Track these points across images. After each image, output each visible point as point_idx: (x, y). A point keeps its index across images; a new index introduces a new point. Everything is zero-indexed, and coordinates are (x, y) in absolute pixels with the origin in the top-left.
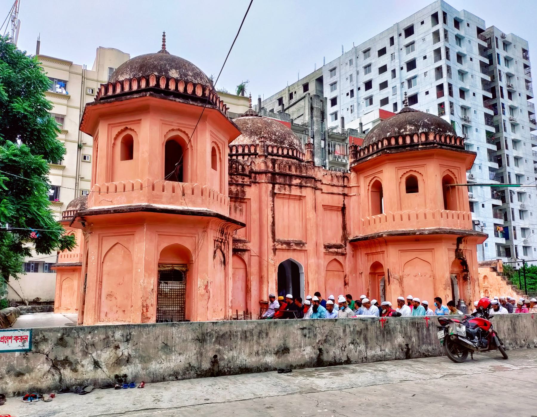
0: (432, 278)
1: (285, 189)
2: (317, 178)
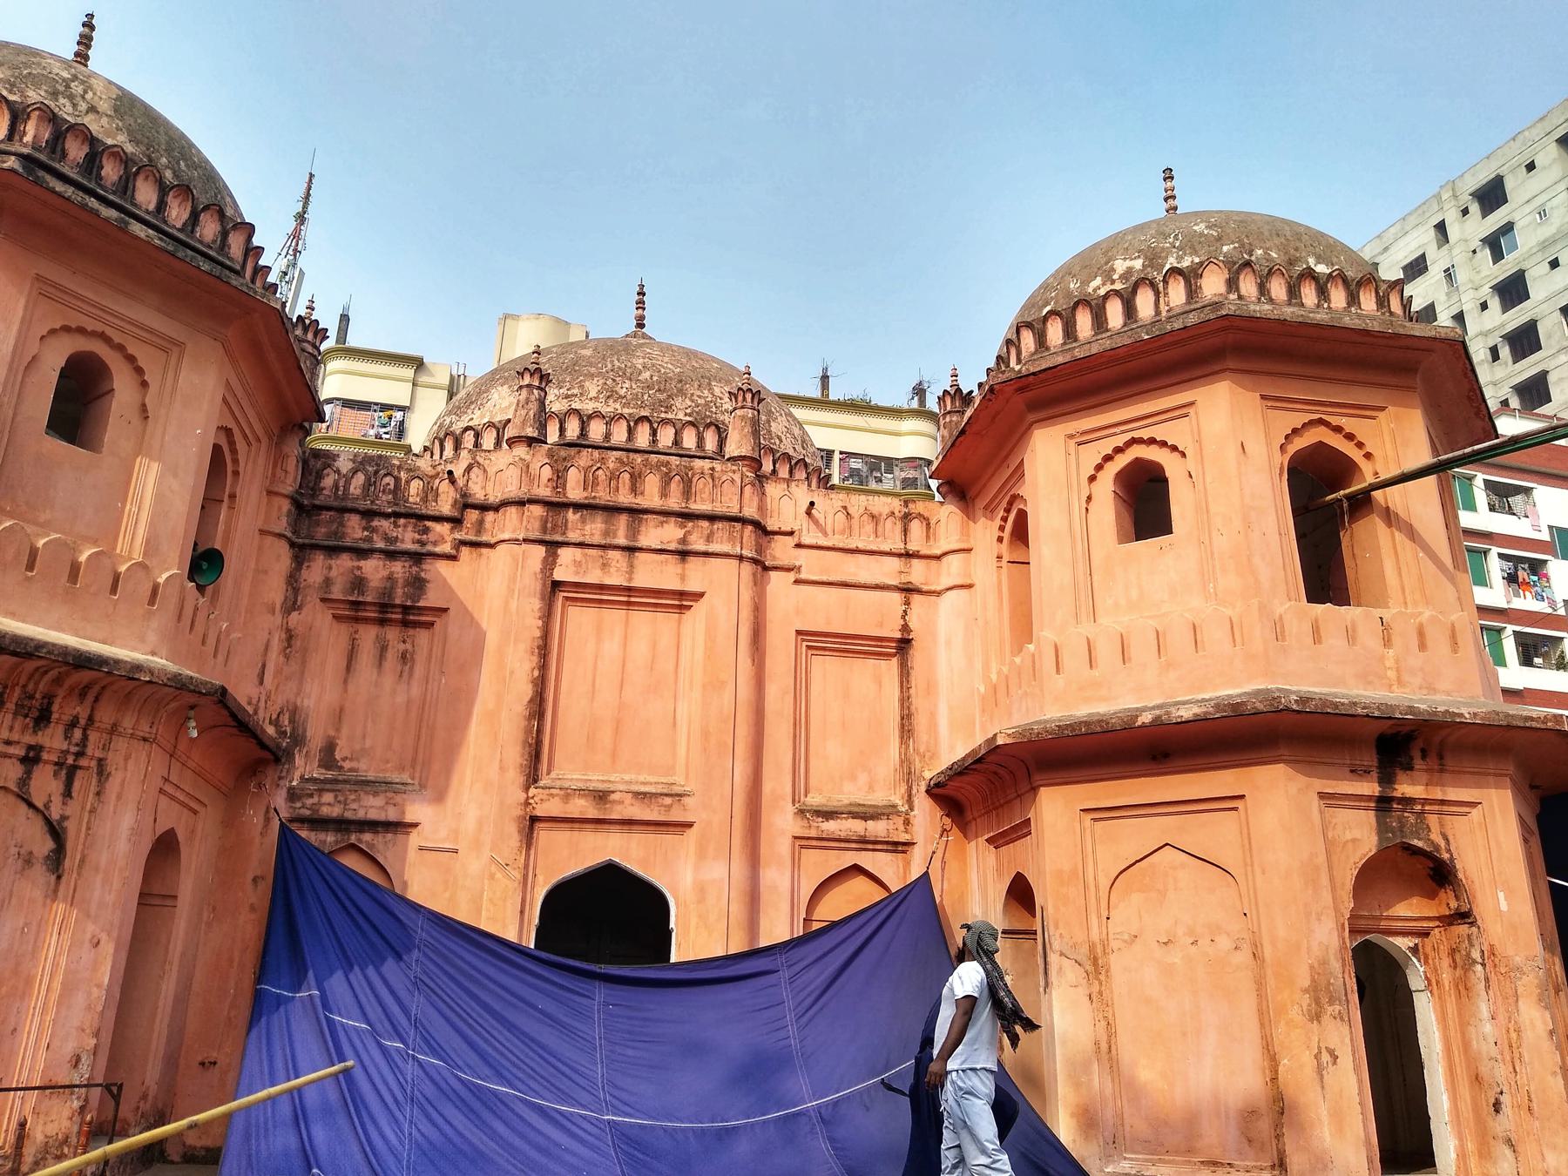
0: (1243, 957)
1: (605, 566)
2: (771, 525)
